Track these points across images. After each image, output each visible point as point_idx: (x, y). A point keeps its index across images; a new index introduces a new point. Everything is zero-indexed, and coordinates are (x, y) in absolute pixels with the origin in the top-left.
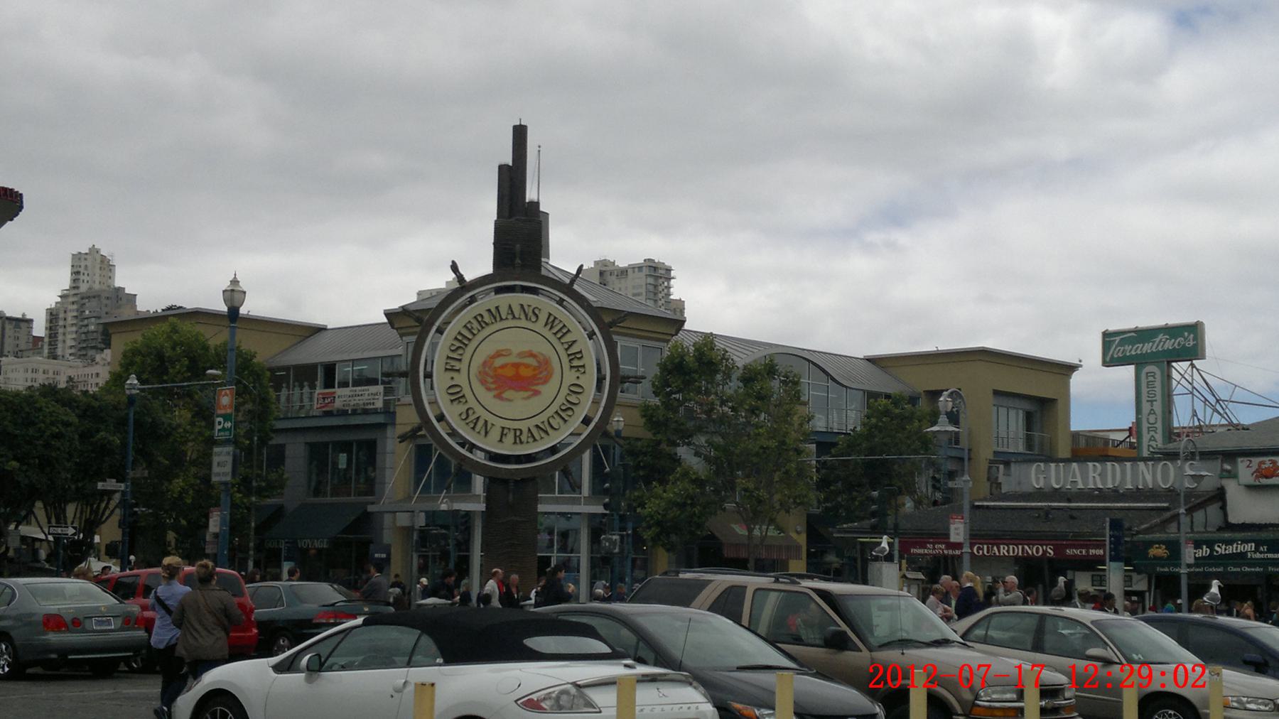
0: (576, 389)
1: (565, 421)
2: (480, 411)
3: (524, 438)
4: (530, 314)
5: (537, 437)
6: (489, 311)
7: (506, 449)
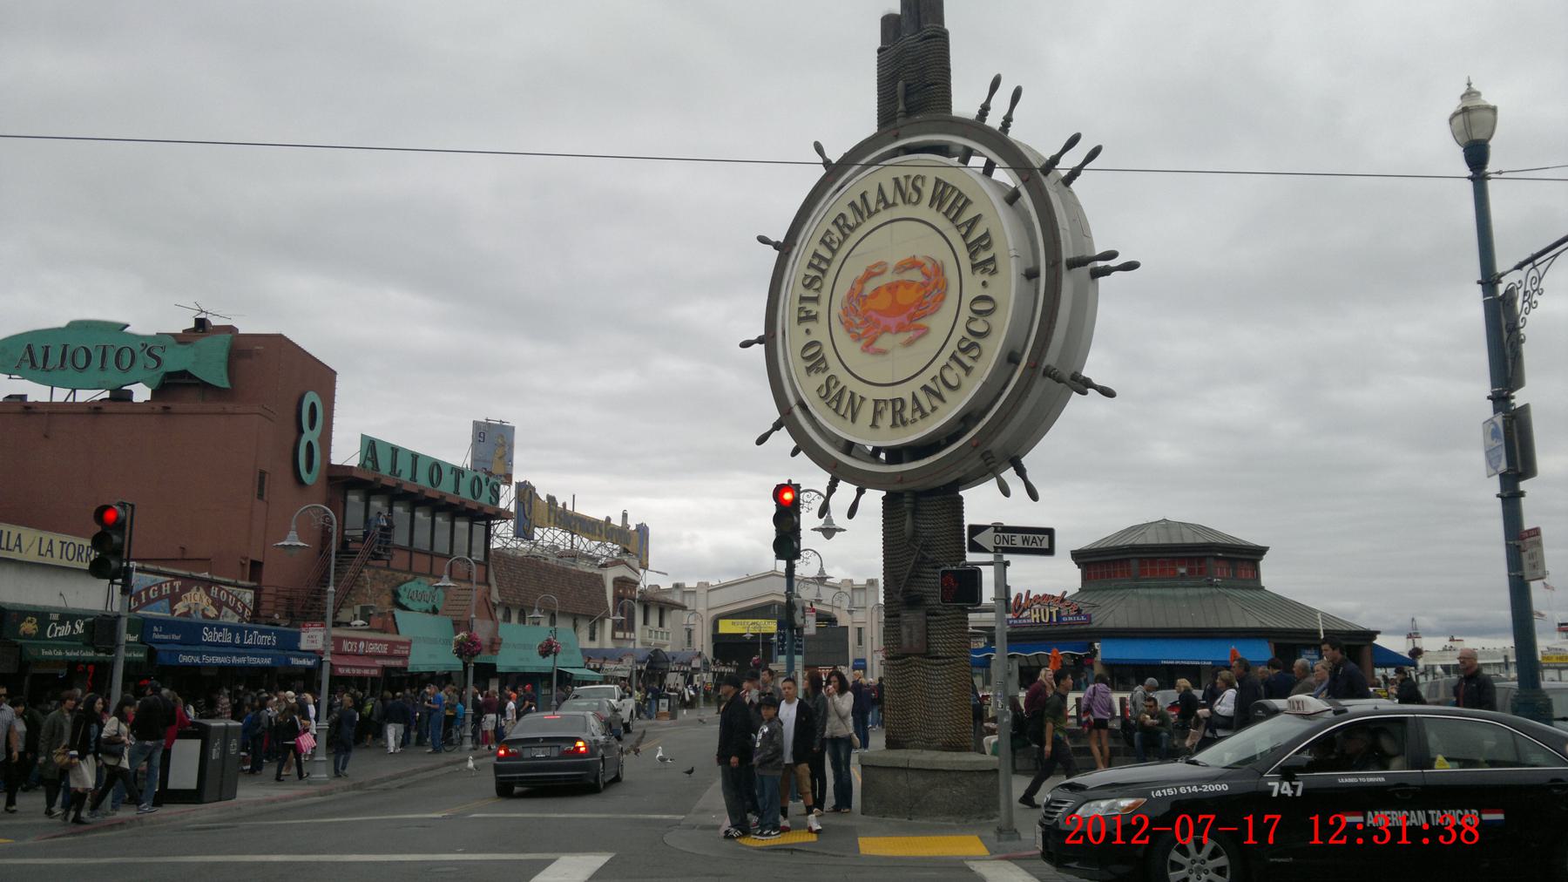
0: (984, 306)
1: (968, 370)
4: (910, 189)
5: (927, 408)
6: (852, 205)
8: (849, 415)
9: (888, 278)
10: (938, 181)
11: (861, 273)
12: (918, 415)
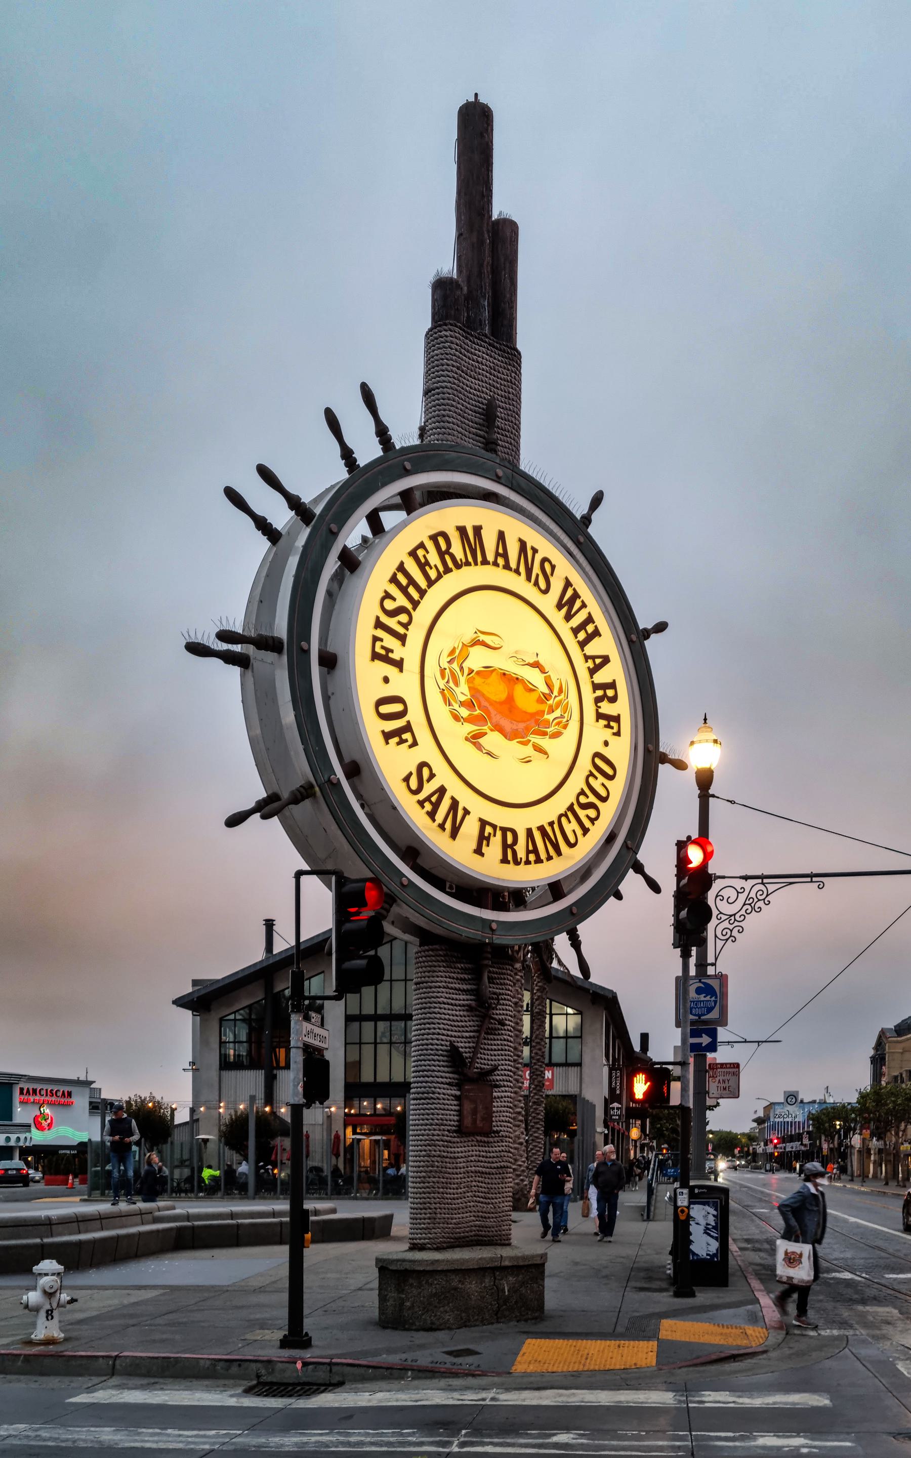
5: (543, 856)
8: (448, 825)
12: (532, 857)
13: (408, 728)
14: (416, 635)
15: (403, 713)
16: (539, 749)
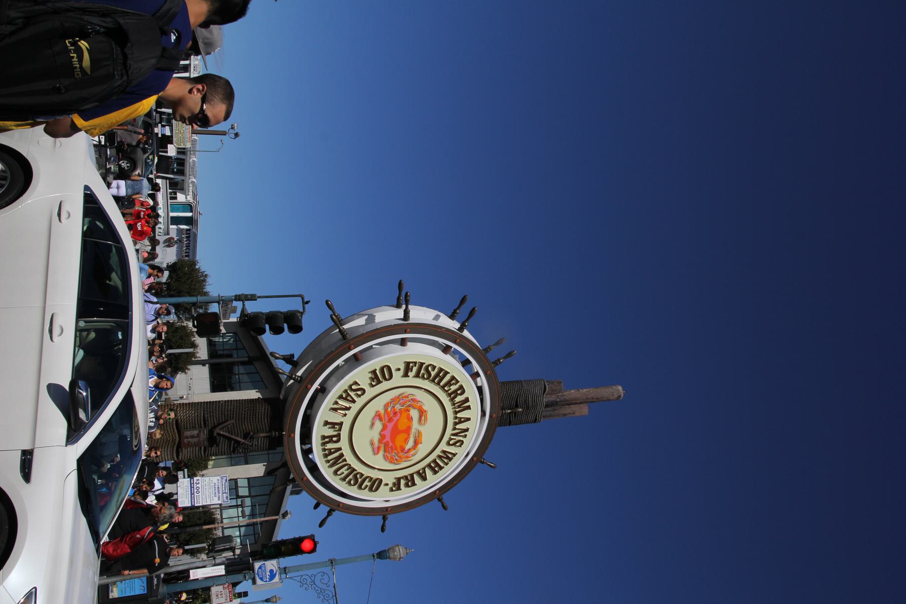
2: (360, 402)
3: (329, 446)
4: (458, 438)
5: (329, 458)
7: (318, 431)
9: (415, 425)
10: (454, 455)
11: (425, 408)
13: (379, 382)
14: (419, 382)
15: (386, 380)
16: (379, 448)
